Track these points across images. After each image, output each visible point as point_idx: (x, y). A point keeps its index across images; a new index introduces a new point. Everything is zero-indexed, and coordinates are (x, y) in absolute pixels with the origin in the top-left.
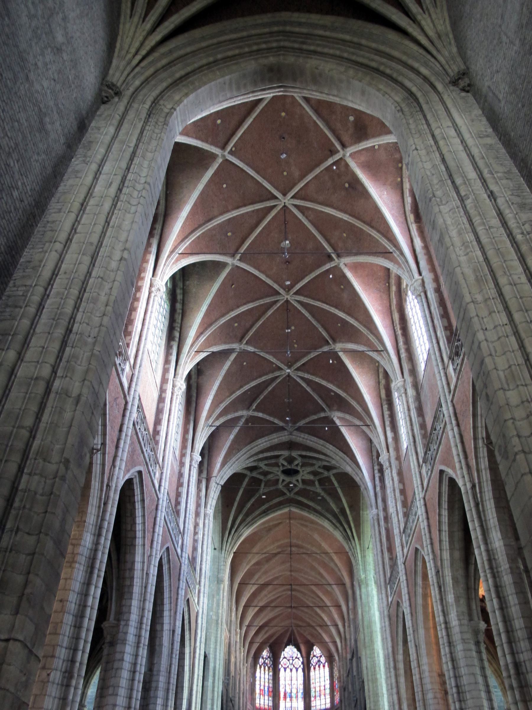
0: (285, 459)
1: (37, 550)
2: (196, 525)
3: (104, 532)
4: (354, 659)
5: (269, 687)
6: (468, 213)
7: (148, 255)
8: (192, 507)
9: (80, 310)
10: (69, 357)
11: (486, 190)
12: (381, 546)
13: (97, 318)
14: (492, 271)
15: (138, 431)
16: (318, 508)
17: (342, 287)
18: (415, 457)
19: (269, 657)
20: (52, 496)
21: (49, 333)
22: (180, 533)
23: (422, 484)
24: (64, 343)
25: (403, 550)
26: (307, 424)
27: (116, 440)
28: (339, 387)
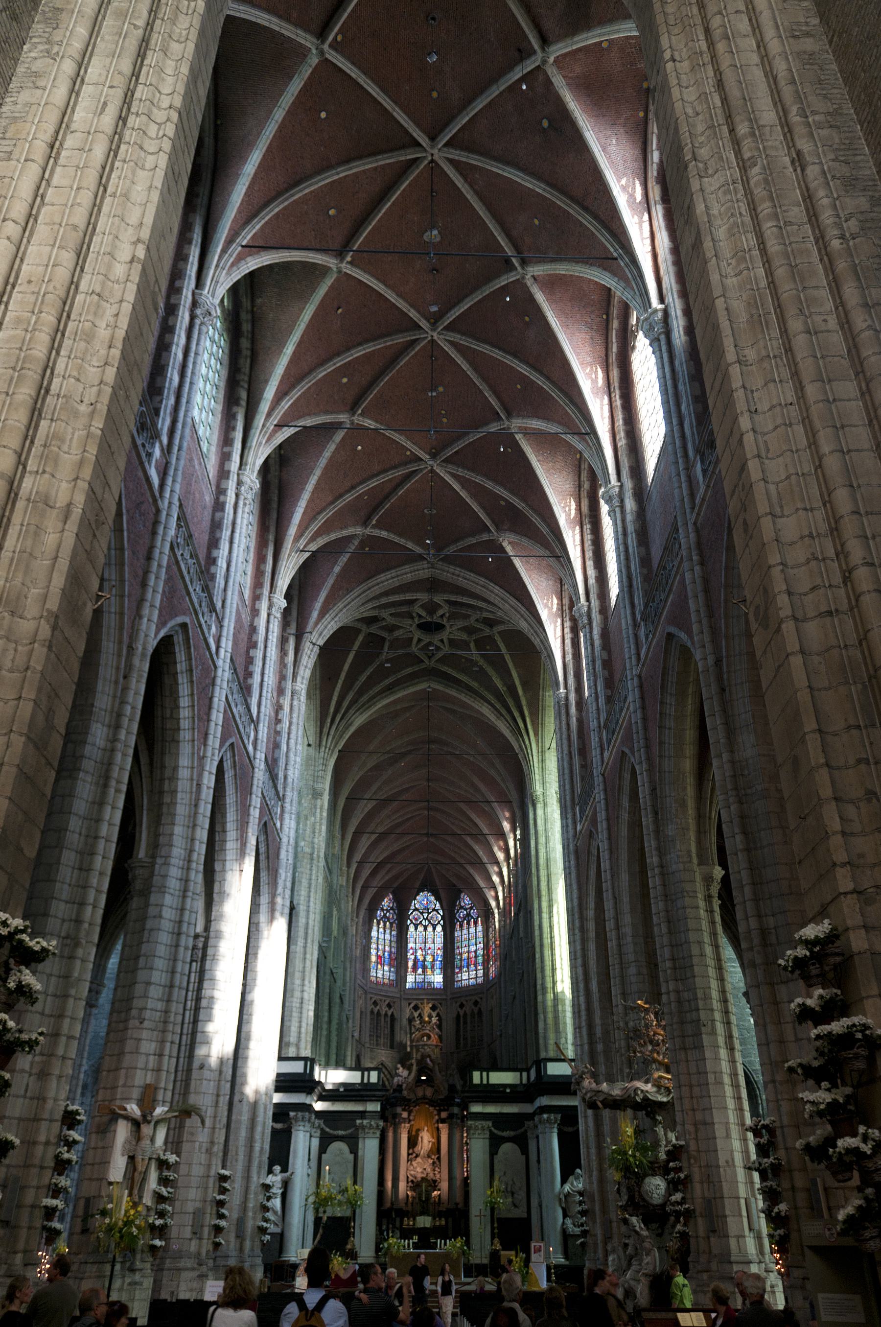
0: (422, 606)
1: (6, 759)
2: (278, 708)
3: (125, 721)
4: (521, 914)
5: (390, 952)
6: (752, 194)
7: (186, 246)
8: (271, 679)
9: (63, 353)
10: (47, 436)
11: (789, 148)
12: (570, 746)
13: (95, 369)
14: (779, 307)
15: (180, 558)
16: (475, 685)
17: (527, 319)
18: (628, 612)
19: (392, 908)
20: (29, 672)
21: (7, 394)
22: (253, 721)
23: (638, 654)
24: (36, 413)
25: (602, 754)
26: (461, 550)
27: (140, 573)
28: (512, 492)
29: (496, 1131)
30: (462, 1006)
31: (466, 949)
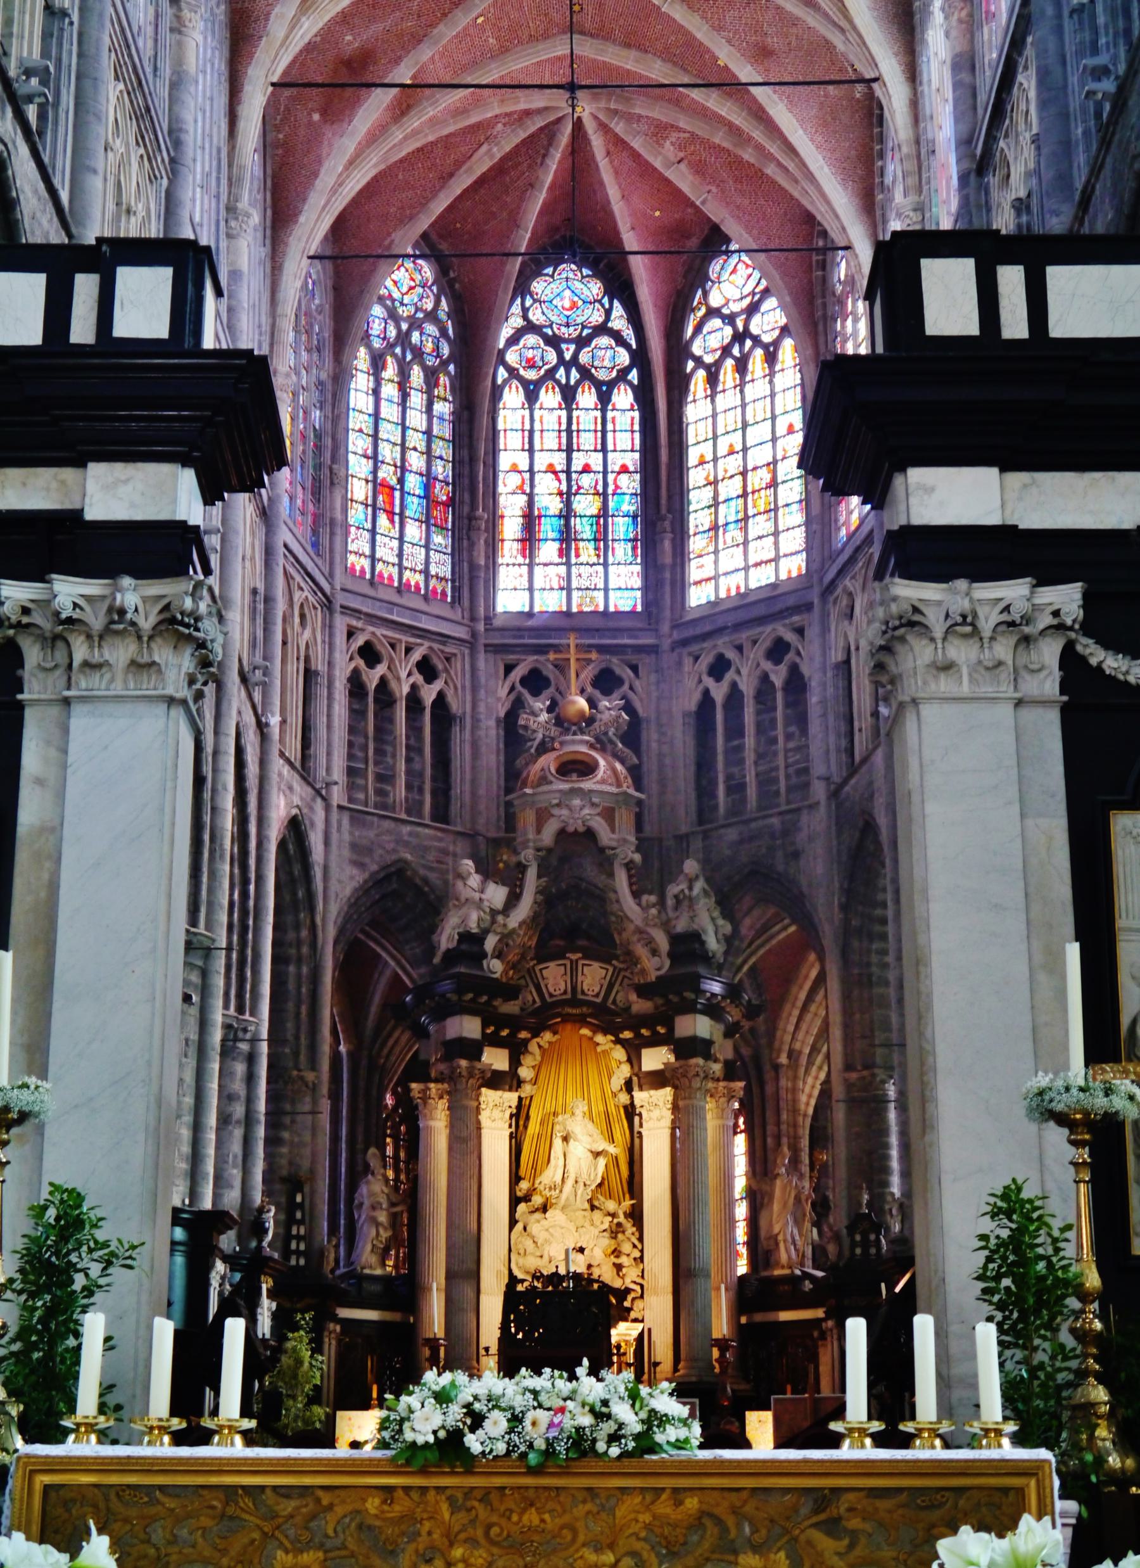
19: (432, 316)
29: (1113, 663)
30: (719, 668)
31: (733, 464)
